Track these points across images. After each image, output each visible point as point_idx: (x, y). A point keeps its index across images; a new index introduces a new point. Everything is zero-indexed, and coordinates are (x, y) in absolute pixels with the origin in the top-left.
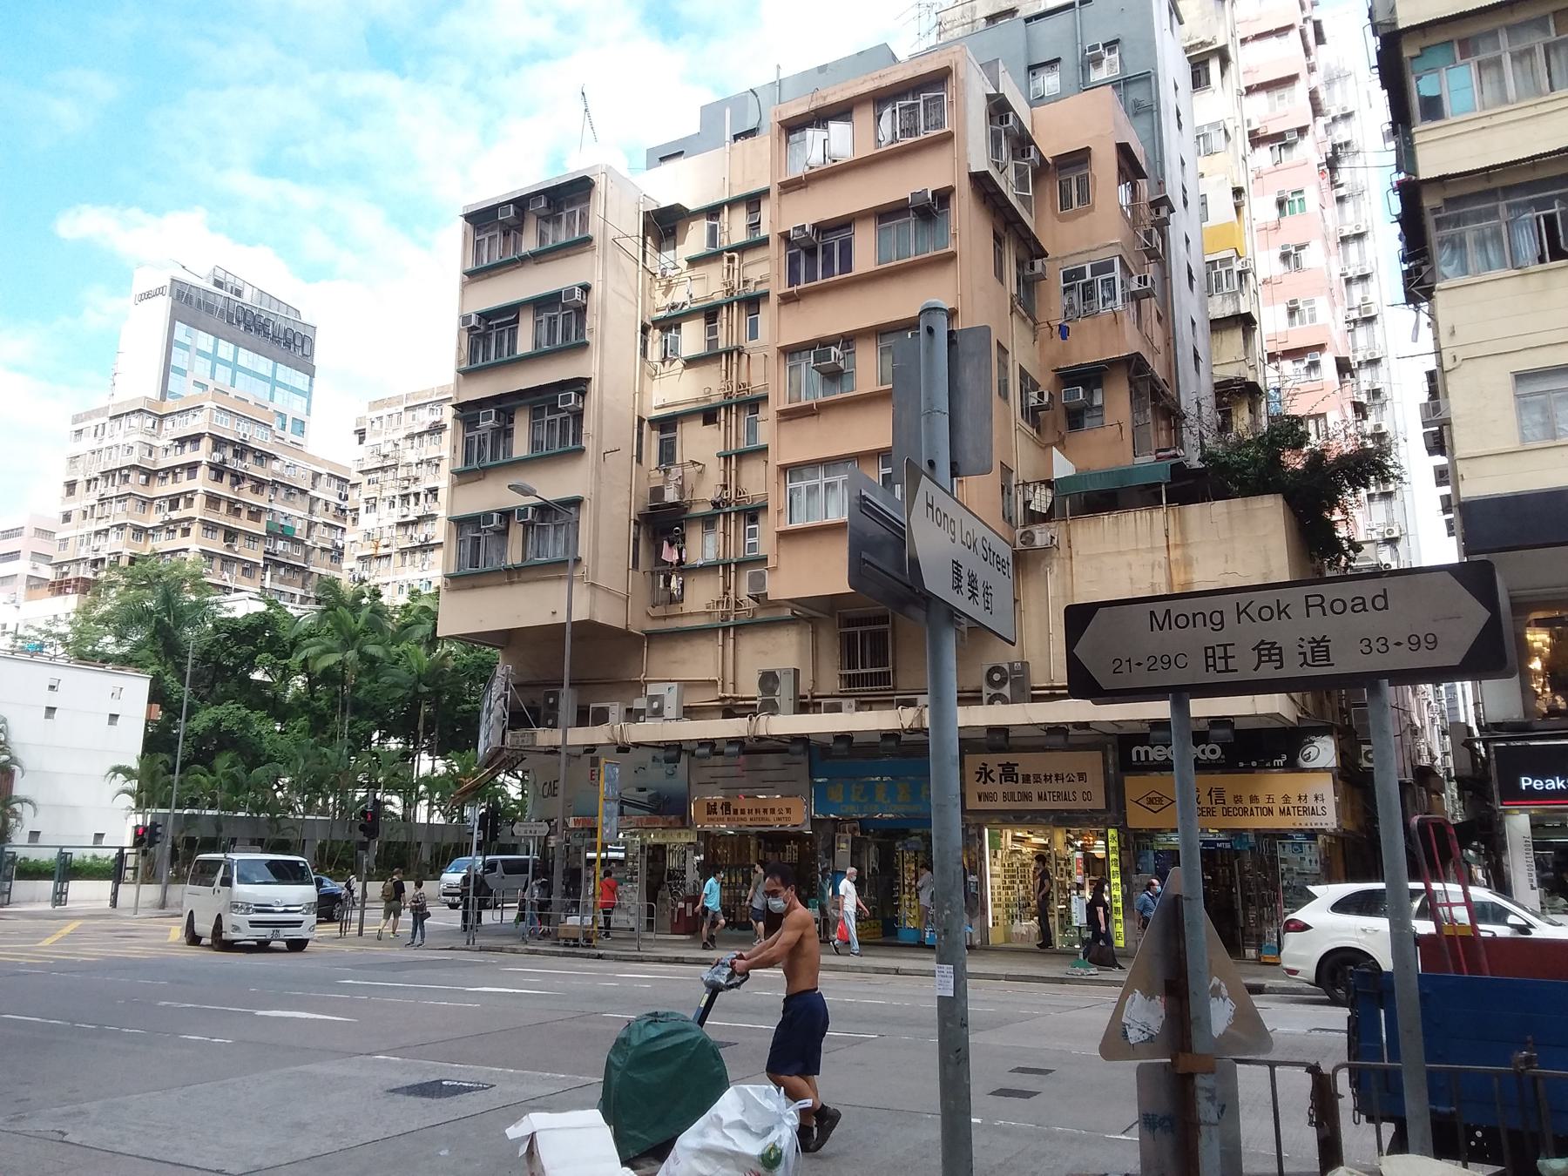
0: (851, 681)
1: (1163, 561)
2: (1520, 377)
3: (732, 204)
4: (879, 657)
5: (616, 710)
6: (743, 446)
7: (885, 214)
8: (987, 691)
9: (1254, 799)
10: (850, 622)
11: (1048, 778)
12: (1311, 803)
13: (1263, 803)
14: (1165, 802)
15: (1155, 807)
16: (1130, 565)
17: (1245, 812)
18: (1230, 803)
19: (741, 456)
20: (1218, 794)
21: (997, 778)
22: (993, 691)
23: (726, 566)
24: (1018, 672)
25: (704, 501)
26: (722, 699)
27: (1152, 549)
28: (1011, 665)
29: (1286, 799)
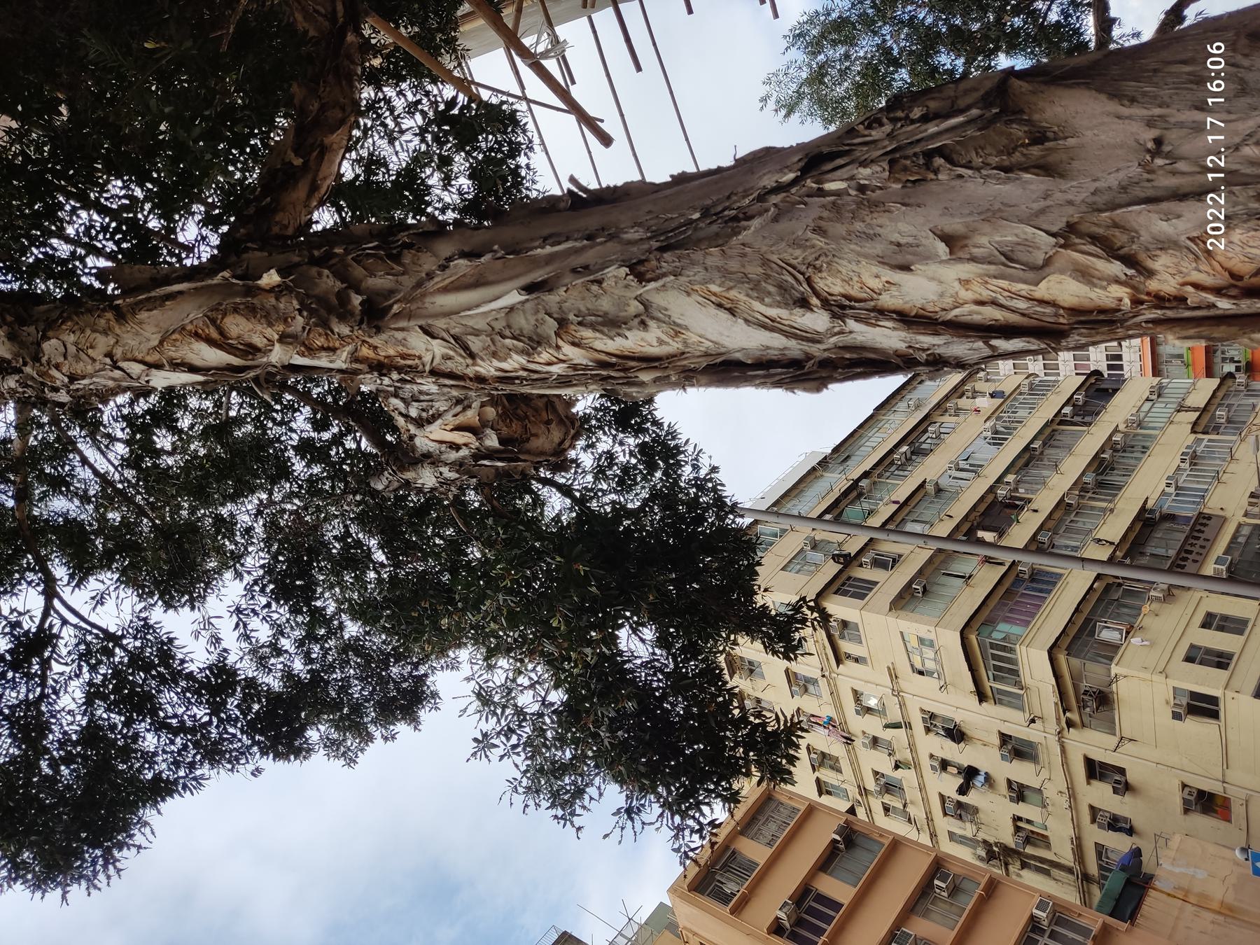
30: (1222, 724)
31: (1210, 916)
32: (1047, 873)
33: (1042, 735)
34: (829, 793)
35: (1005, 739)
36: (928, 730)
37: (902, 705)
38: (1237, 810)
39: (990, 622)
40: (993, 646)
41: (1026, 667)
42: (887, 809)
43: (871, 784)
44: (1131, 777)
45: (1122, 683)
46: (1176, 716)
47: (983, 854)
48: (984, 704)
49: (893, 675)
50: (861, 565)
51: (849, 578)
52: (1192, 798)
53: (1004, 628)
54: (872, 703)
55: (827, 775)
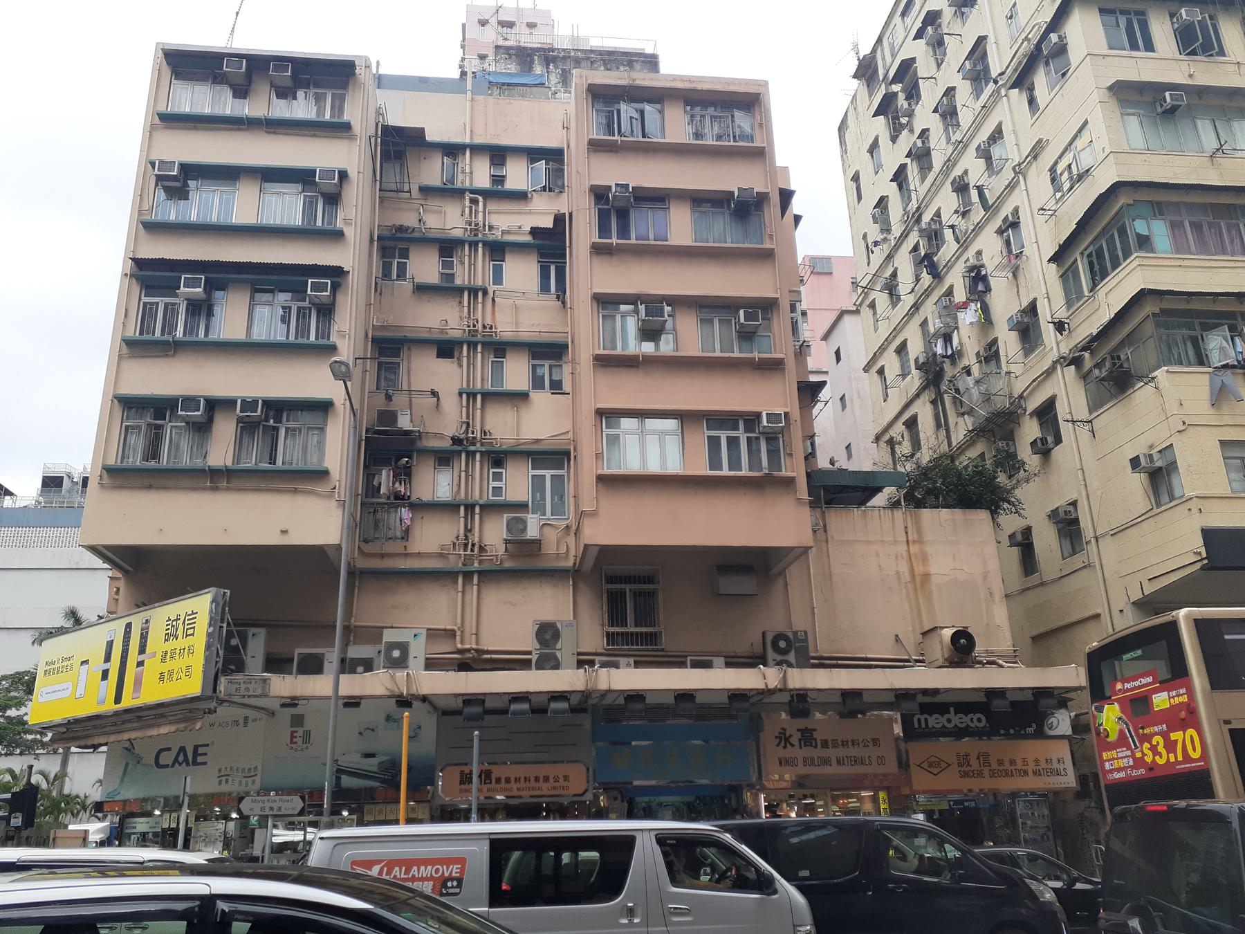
0: (611, 638)
1: (905, 554)
2: (1223, 444)
3: (477, 149)
4: (646, 614)
5: (332, 657)
6: (489, 387)
7: (700, 200)
8: (771, 654)
9: (1013, 762)
10: (611, 580)
11: (845, 743)
12: (1055, 766)
13: (1019, 766)
14: (944, 765)
15: (935, 771)
16: (878, 555)
17: (1007, 774)
18: (994, 766)
19: (487, 396)
20: (984, 757)
21: (797, 744)
22: (779, 658)
23: (470, 507)
24: (802, 641)
25: (440, 436)
26: (459, 651)
27: (895, 542)
28: (795, 633)
29: (1037, 761)
30: (1156, 511)
31: (904, 567)
32: (938, 426)
33: (1053, 344)
34: (900, 187)
35: (1032, 309)
36: (1000, 232)
37: (1011, 186)
38: (1078, 561)
39: (1159, 209)
40: (1123, 232)
41: (1117, 280)
42: (916, 248)
43: (926, 218)
44: (1057, 452)
45: (1149, 389)
46: (1135, 462)
47: (921, 361)
48: (1053, 266)
49: (1037, 150)
50: (1172, 16)
51: (1143, 13)
52: (1062, 515)
53: (1159, 231)
54: (996, 152)
55: (913, 172)
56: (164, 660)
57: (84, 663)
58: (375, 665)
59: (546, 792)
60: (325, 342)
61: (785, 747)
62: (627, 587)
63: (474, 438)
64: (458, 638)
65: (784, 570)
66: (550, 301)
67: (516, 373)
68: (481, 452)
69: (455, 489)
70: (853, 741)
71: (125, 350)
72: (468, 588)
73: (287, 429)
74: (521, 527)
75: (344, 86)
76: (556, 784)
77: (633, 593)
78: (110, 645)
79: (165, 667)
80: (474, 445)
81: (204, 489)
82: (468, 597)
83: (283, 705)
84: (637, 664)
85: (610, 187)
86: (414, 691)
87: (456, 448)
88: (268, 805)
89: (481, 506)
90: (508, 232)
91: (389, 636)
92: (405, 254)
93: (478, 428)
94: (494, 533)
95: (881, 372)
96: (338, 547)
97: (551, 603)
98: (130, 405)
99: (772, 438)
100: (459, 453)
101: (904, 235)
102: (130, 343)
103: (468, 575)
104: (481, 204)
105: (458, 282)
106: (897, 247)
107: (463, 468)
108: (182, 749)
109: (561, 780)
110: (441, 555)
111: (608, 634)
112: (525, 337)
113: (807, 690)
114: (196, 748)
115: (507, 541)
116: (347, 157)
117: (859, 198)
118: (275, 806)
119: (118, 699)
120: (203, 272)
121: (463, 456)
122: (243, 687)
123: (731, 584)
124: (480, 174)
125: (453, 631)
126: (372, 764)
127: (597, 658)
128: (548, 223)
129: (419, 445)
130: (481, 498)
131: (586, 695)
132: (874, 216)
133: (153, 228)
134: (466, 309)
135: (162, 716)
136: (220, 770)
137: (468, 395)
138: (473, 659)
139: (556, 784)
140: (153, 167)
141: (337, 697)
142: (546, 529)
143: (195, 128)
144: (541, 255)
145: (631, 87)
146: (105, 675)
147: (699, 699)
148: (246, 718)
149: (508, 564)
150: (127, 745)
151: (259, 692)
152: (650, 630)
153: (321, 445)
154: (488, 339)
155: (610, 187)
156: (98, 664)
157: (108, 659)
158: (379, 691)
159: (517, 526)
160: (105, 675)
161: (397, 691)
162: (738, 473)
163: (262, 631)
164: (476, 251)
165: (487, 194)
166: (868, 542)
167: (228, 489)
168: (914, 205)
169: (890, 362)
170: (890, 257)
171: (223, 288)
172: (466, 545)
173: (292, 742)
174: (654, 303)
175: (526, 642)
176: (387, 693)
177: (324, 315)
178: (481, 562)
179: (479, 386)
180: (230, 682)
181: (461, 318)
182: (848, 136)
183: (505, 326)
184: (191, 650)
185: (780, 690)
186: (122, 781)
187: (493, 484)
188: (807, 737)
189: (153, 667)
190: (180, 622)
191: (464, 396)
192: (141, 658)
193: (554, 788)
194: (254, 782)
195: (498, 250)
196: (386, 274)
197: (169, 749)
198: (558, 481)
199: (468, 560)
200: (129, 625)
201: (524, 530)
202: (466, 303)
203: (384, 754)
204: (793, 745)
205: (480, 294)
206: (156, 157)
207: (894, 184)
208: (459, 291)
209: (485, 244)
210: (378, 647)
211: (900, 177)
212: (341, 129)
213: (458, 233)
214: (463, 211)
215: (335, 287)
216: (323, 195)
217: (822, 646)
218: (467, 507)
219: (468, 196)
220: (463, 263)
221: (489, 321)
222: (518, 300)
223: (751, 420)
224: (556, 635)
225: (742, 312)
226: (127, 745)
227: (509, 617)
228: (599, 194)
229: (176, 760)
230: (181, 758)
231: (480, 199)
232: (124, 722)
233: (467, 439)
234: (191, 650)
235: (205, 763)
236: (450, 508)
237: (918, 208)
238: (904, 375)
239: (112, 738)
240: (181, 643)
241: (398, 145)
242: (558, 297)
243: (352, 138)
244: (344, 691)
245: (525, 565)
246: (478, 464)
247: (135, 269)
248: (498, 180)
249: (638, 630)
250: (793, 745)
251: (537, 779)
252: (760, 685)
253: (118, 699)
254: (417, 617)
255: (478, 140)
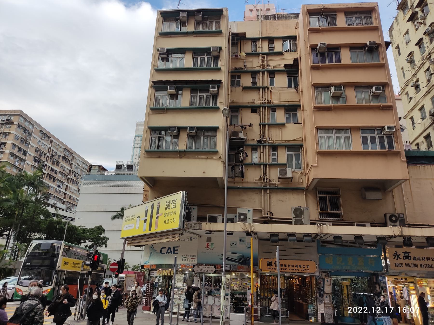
0: (321, 215)
3: (264, 39)
5: (220, 217)
6: (270, 122)
7: (353, 48)
8: (389, 222)
10: (320, 193)
11: (423, 259)
16: (431, 183)
19: (270, 125)
23: (265, 165)
24: (402, 217)
26: (263, 218)
28: (399, 214)
34: (420, 47)
42: (428, 70)
56: (165, 216)
57: (138, 217)
58: (235, 221)
59: (288, 271)
60: (215, 106)
61: (397, 259)
62: (327, 196)
63: (265, 141)
64: (263, 213)
65: (392, 190)
66: (293, 91)
67: (280, 116)
68: (268, 146)
69: (259, 159)
70: (427, 258)
71: (151, 112)
72: (265, 194)
73: (204, 137)
74: (285, 172)
75: (220, 18)
76: (304, 269)
77: (330, 198)
78: (147, 211)
79: (166, 219)
80: (265, 143)
81: (177, 158)
82: (266, 198)
83: (206, 233)
84: (333, 225)
85: (317, 45)
86: (253, 230)
87: (259, 144)
88: (203, 269)
89: (269, 165)
90: (276, 67)
91: (239, 211)
92: (239, 77)
93: (267, 137)
94: (274, 175)
95: (412, 118)
96: (222, 178)
97: (298, 201)
98: (153, 130)
99: (389, 137)
100: (260, 146)
101: (422, 65)
102: (152, 109)
103: (265, 190)
104: (266, 58)
105: (258, 85)
106: (418, 70)
107: (262, 151)
108: (169, 248)
109: (306, 267)
110: (255, 183)
111: (320, 213)
112: (283, 104)
113: (410, 236)
114: (174, 248)
115: (279, 178)
116: (221, 42)
117: (400, 54)
118: (206, 269)
119: (150, 230)
120: (175, 85)
121: (262, 147)
122: (193, 226)
123: (371, 195)
124: (265, 47)
125: (261, 210)
126: (235, 257)
127: (317, 222)
128: (291, 62)
129: (246, 143)
130: (269, 162)
131: (317, 235)
132: (407, 60)
133: (159, 71)
134: (261, 95)
135: (164, 236)
136: (183, 256)
137: (263, 125)
138: (269, 220)
139: (304, 269)
140: (158, 51)
141: (226, 231)
142: (294, 173)
143: (171, 37)
144: (288, 74)
145: (324, 9)
146: (145, 221)
147: (365, 239)
148: (191, 238)
149: (280, 186)
150: (151, 246)
151: (198, 228)
152: (337, 212)
153: (215, 143)
154: (270, 105)
155: (317, 45)
156: (143, 218)
157: (146, 216)
158: (240, 230)
159: (283, 173)
160: (145, 221)
161: (246, 230)
162: (376, 150)
163: (196, 207)
164: (264, 74)
165: (268, 54)
166: (426, 179)
167: (185, 158)
168: (427, 53)
169: (417, 115)
170: (415, 75)
171: (181, 90)
172: (264, 179)
173: (207, 247)
174: (338, 86)
175: (290, 215)
176: (243, 230)
177: (215, 97)
178: (270, 185)
179: (267, 122)
180: (189, 224)
181: (259, 98)
182: (394, 32)
183: (275, 100)
184: (175, 213)
185: (399, 236)
186: (149, 258)
187: (273, 157)
188: (407, 256)
189: (162, 218)
190: (171, 203)
191: (261, 126)
192: (157, 215)
193: (303, 270)
194: (195, 260)
195: (272, 73)
196: (233, 85)
197: (165, 248)
198: (298, 157)
199: (265, 185)
200: (153, 205)
201: (286, 173)
202: (261, 93)
203: (240, 253)
204: (401, 259)
205: (266, 89)
206: (159, 47)
207: (417, 46)
208: (259, 89)
209: (268, 72)
210: (235, 215)
211: (420, 43)
212: (219, 33)
213: (258, 69)
214: (259, 61)
215: (219, 87)
216: (213, 56)
217: (409, 220)
218: (264, 165)
219: (261, 55)
220: (259, 79)
221: (269, 99)
222: (280, 91)
223: (382, 128)
224: (302, 213)
225: (374, 88)
226: (151, 246)
227: (283, 205)
228: (313, 48)
229: (167, 252)
230: (169, 251)
231: (265, 56)
232: (151, 238)
233: (263, 141)
234: (175, 213)
235: (177, 253)
236: (257, 165)
237: (429, 54)
238: (423, 119)
239: (148, 243)
240: (171, 210)
241: (237, 39)
242: (295, 89)
243: (223, 36)
244: (228, 229)
245: (287, 186)
246: (267, 150)
247: (153, 85)
248: (271, 49)
249: (332, 212)
250: (401, 259)
251: (296, 266)
252: (391, 234)
253: (150, 230)
254: (249, 205)
255: (264, 36)
